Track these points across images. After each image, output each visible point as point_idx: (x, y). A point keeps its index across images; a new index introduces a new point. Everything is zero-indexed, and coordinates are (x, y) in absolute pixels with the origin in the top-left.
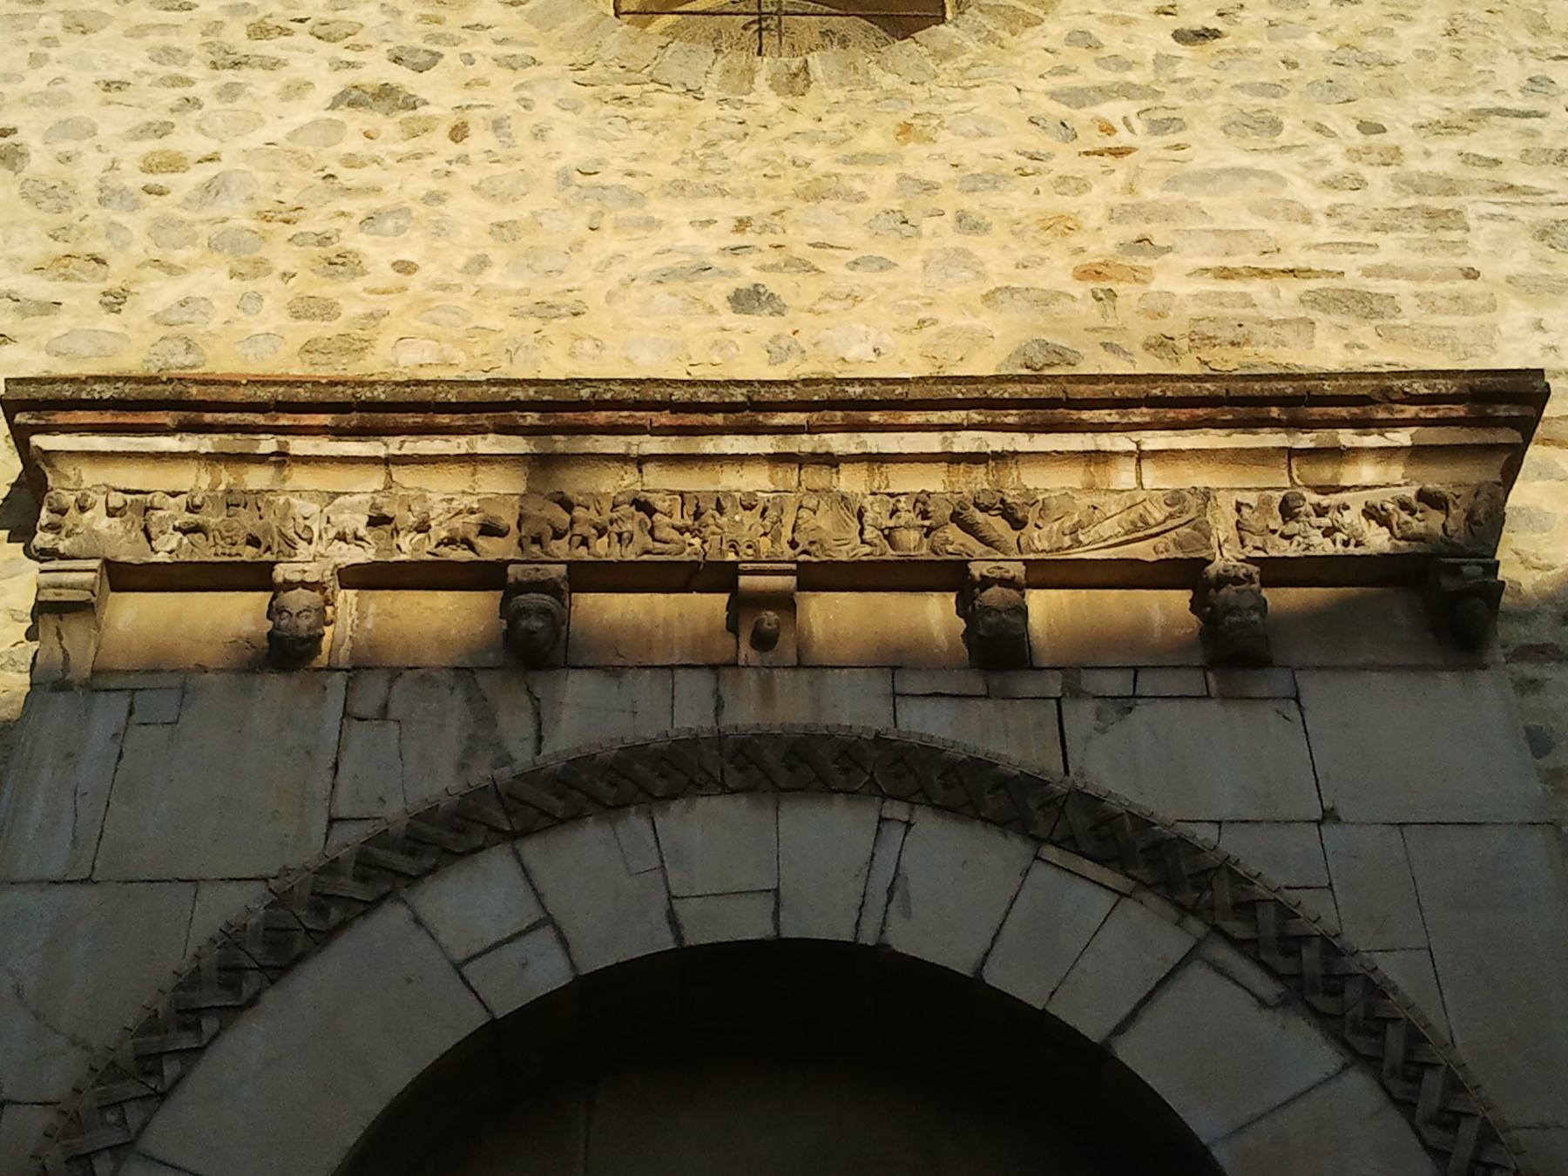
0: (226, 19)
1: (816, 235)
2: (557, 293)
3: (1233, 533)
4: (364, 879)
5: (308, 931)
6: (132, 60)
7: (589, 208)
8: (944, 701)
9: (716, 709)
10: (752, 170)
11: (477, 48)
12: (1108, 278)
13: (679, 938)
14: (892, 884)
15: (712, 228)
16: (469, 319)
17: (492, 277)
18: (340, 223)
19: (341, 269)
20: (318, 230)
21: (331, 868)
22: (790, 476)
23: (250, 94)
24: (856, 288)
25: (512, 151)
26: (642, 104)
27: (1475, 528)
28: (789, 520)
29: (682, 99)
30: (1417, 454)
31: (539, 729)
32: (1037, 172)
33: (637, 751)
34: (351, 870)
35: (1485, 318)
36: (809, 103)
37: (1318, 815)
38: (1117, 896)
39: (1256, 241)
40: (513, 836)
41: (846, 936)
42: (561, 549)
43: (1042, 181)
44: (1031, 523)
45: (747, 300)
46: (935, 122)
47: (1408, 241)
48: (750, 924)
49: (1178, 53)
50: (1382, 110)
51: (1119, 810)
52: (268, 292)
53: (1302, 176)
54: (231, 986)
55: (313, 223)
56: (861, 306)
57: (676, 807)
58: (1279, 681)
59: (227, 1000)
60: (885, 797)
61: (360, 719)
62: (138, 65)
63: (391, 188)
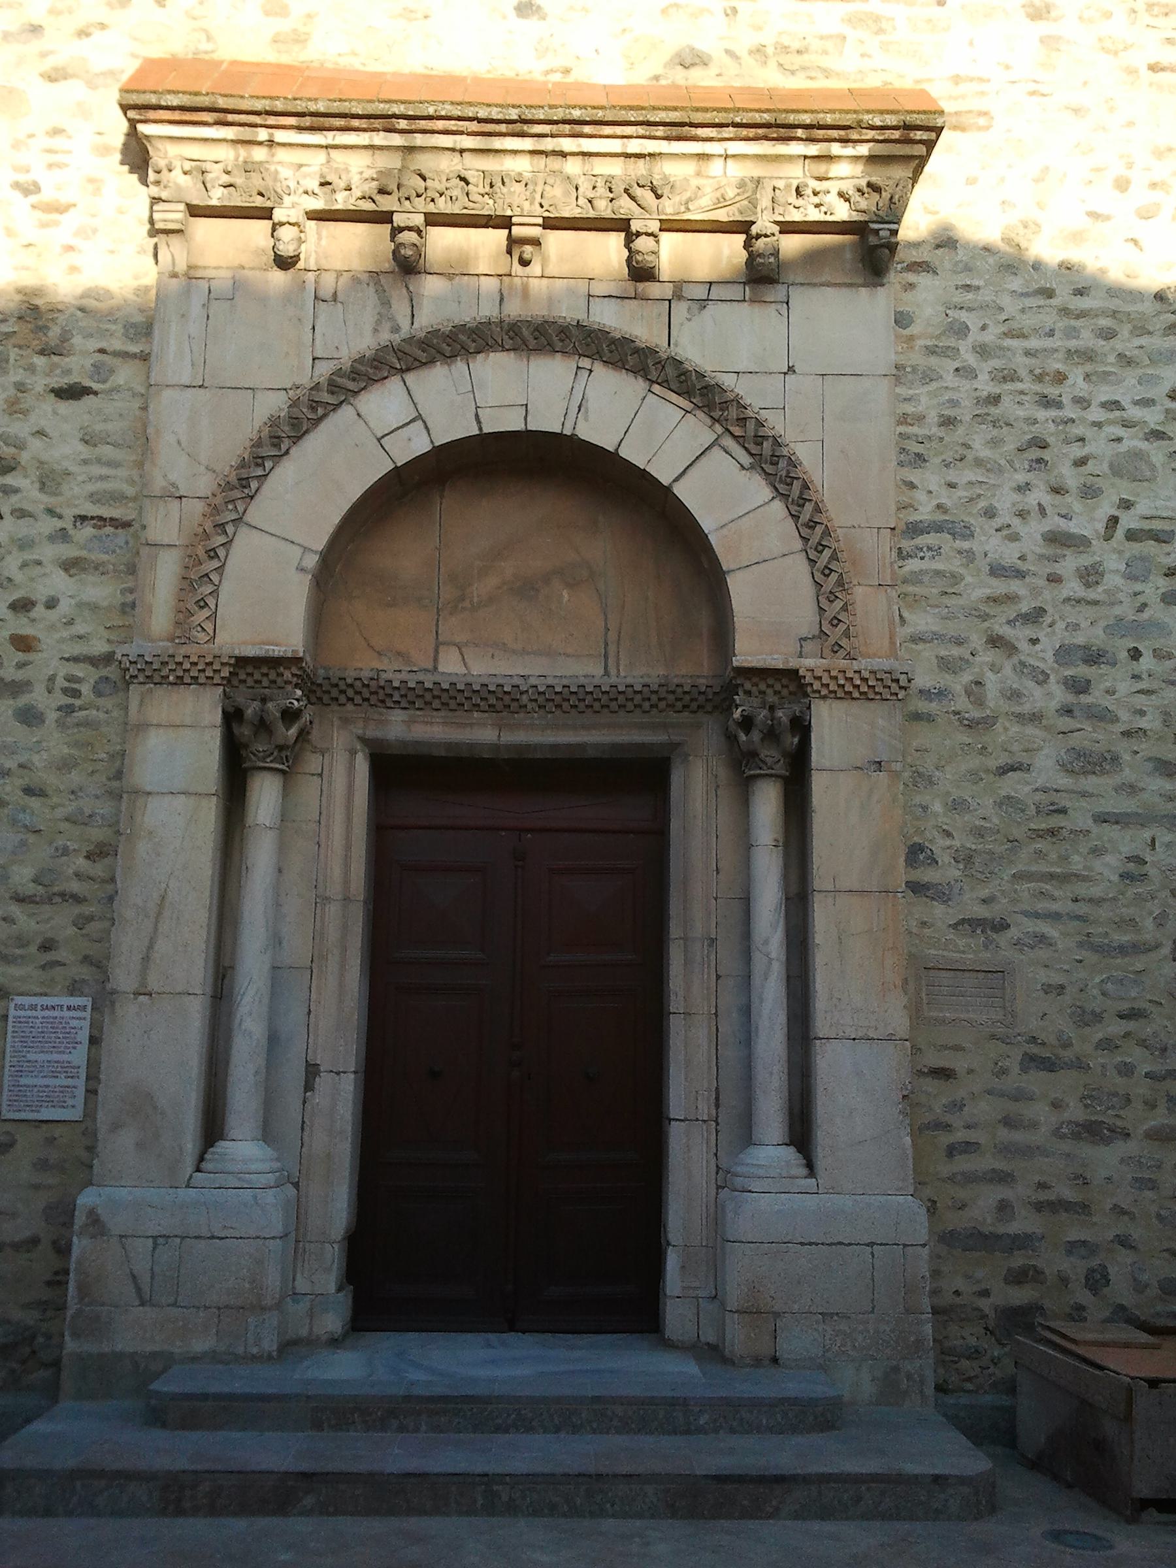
3: (770, 204)
4: (333, 393)
5: (308, 419)
8: (614, 300)
22: (541, 161)
27: (892, 206)
28: (539, 189)
30: (872, 159)
31: (412, 311)
33: (462, 328)
38: (684, 412)
42: (420, 204)
48: (513, 422)
51: (691, 369)
54: (277, 446)
57: (480, 357)
58: (779, 292)
60: (580, 355)
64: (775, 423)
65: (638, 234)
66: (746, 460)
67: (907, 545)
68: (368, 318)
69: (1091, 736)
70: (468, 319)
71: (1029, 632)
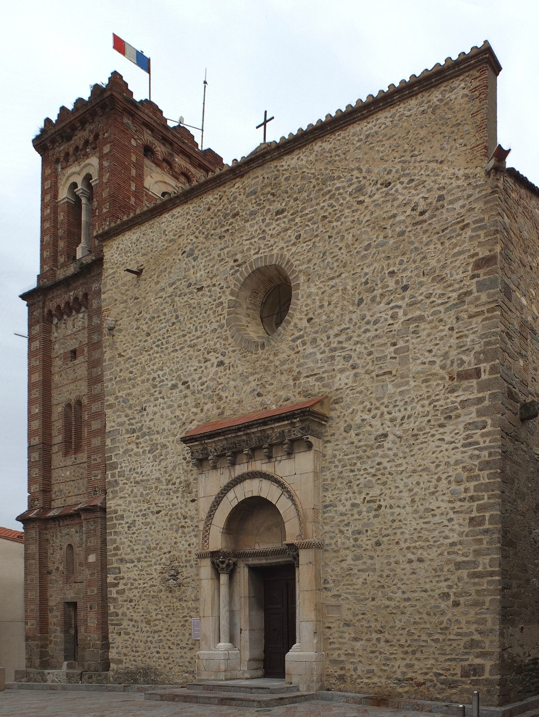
45: (259, 395)
67: (324, 510)
69: (358, 551)
71: (347, 528)
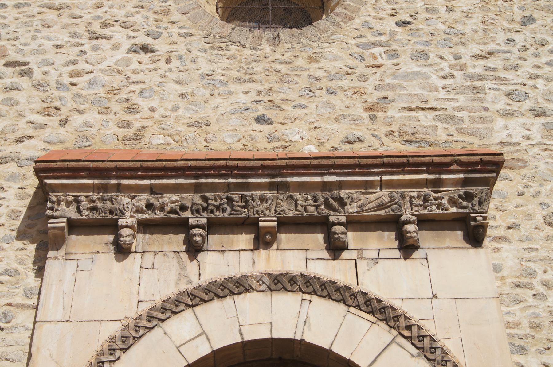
0: (93, 21)
1: (282, 96)
2: (201, 118)
4: (149, 321)
6: (64, 37)
7: (210, 87)
8: (322, 261)
9: (253, 264)
10: (262, 73)
11: (173, 30)
12: (375, 110)
13: (242, 338)
14: (305, 321)
15: (249, 94)
16: (173, 128)
17: (180, 113)
18: (132, 94)
19: (133, 110)
20: (125, 97)
21: (139, 318)
23: (102, 49)
24: (295, 115)
25: (186, 68)
26: (226, 50)
29: (239, 48)
32: (352, 73)
33: (229, 280)
34: (145, 319)
35: (489, 125)
36: (279, 49)
37: (431, 296)
38: (372, 323)
39: (420, 98)
40: (192, 306)
41: (291, 336)
43: (353, 77)
44: (348, 204)
46: (320, 56)
47: (467, 97)
48: (263, 334)
49: (397, 30)
50: (461, 50)
52: (111, 119)
53: (435, 74)
55: (123, 95)
56: (297, 121)
59: (112, 358)
60: (303, 293)
61: (145, 269)
62: (66, 39)
63: (147, 81)
64: (430, 328)
65: (334, 224)
66: (415, 351)
68: (173, 276)
70: (233, 274)
